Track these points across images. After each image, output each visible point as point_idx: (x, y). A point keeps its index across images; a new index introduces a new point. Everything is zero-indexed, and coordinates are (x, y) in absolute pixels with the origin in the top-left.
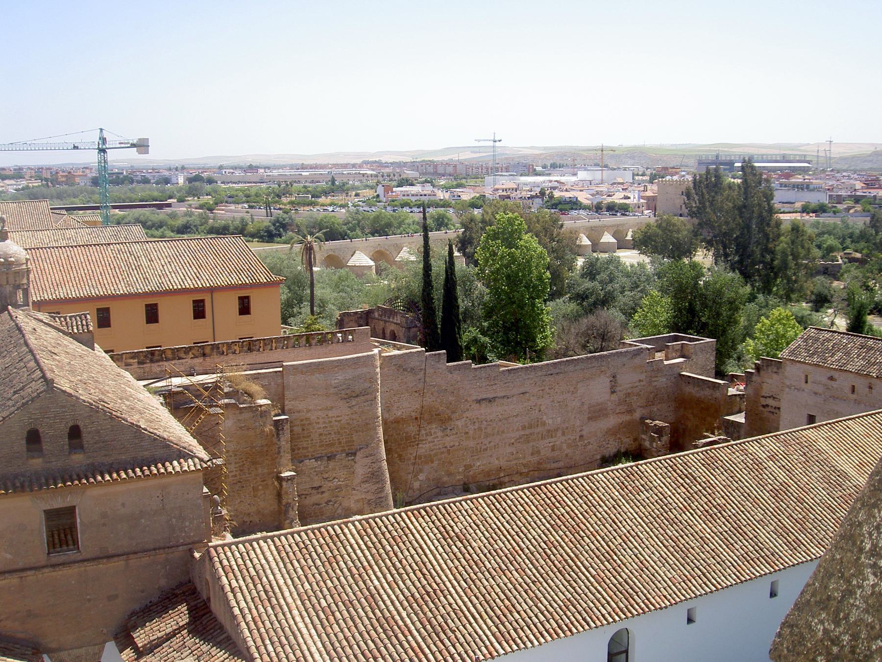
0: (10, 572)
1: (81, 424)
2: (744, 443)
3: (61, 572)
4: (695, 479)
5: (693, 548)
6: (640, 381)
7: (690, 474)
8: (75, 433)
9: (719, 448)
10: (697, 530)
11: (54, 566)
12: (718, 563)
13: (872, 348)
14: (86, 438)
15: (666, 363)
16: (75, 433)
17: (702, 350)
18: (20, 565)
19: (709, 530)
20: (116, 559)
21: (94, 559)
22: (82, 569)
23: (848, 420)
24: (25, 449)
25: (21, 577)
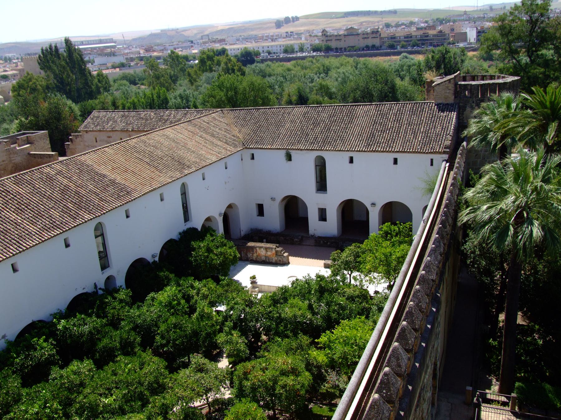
2: (41, 168)
4: (9, 192)
5: (10, 230)
6: (3, 161)
7: (6, 190)
9: (24, 173)
10: (12, 219)
12: (27, 234)
13: (128, 116)
15: (18, 148)
17: (40, 138)
19: (20, 218)
23: (105, 147)
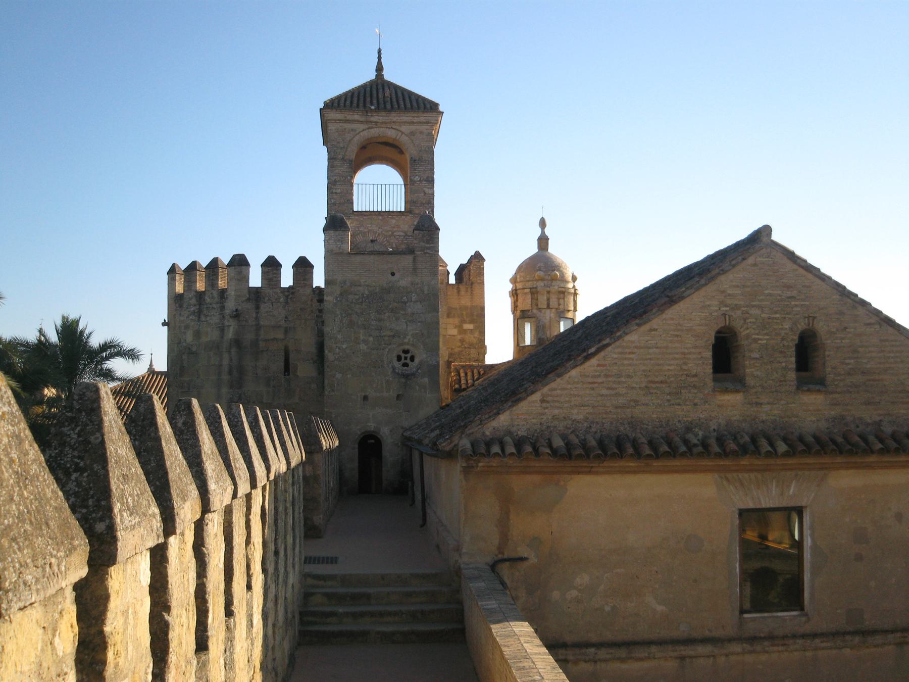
0: (661, 643)
1: (821, 327)
3: (763, 657)
8: (806, 350)
11: (753, 639)
14: (832, 361)
16: (806, 350)
18: (683, 631)
20: (878, 639)
21: (835, 634)
22: (809, 654)
24: (709, 369)
25: (682, 658)
